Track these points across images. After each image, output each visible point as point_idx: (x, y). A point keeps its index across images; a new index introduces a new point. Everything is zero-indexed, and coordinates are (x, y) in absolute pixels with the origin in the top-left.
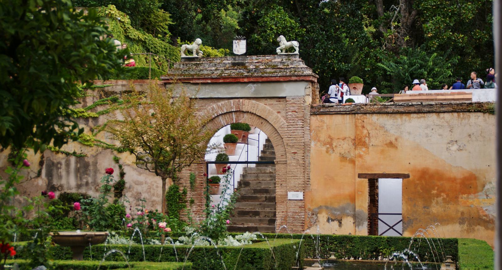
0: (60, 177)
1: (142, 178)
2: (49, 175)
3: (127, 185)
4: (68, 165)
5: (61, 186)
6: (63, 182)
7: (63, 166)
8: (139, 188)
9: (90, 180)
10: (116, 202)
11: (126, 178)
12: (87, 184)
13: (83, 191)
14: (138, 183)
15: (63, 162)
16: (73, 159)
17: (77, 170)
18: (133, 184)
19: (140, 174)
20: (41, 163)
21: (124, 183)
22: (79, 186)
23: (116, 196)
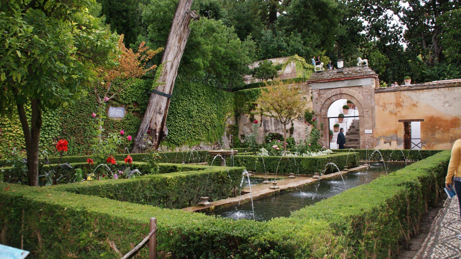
0: (268, 126)
1: (300, 126)
2: (265, 126)
3: (295, 129)
4: (271, 121)
5: (269, 130)
6: (270, 128)
7: (270, 122)
8: (300, 130)
9: (280, 127)
10: (290, 136)
11: (294, 126)
12: (279, 129)
13: (277, 132)
14: (299, 128)
15: (269, 120)
16: (273, 119)
17: (275, 123)
18: (297, 129)
19: (300, 124)
20: (261, 121)
21: (293, 128)
22: (276, 130)
23: (290, 134)
